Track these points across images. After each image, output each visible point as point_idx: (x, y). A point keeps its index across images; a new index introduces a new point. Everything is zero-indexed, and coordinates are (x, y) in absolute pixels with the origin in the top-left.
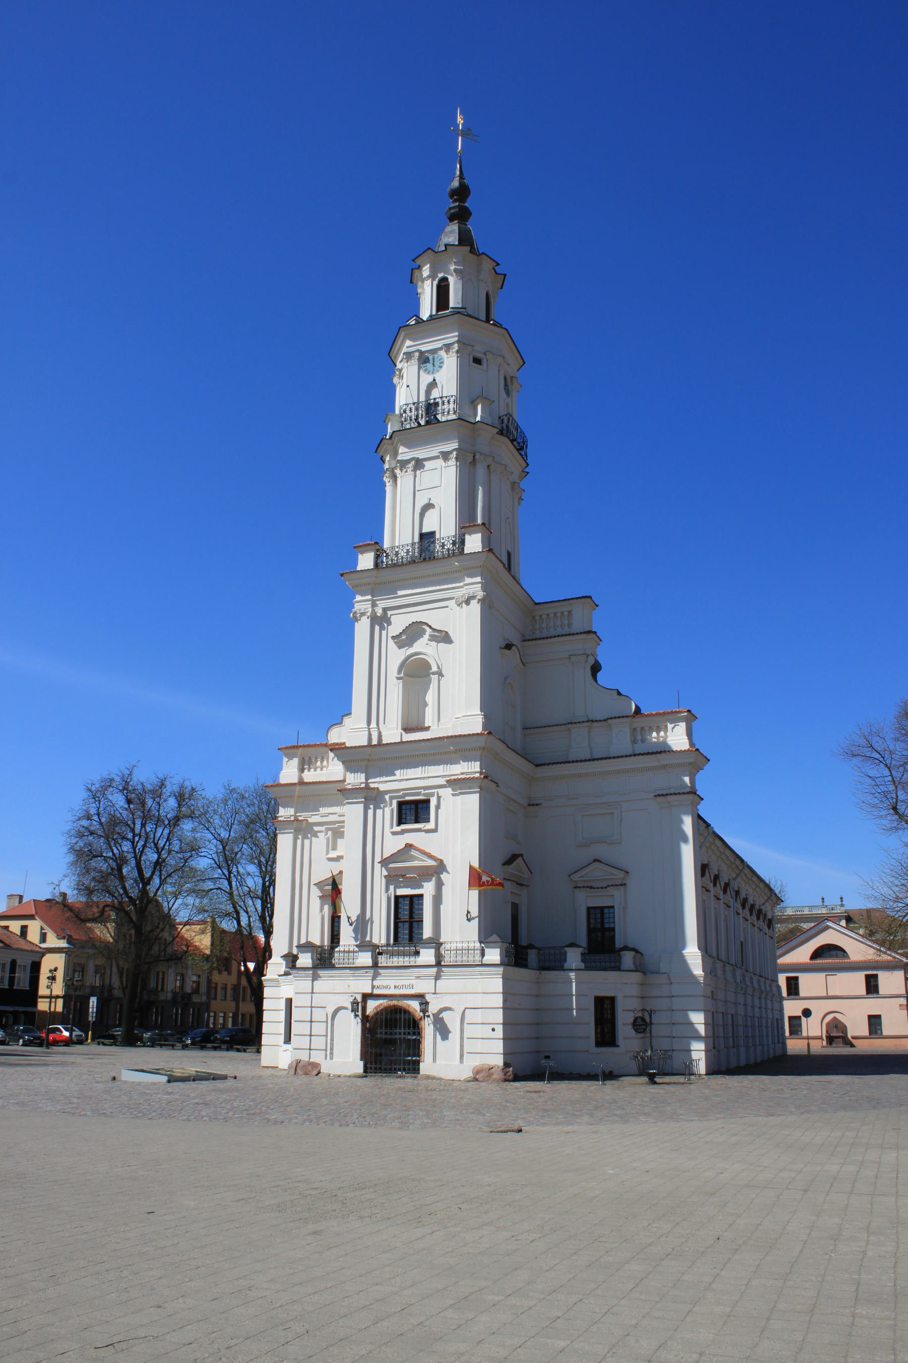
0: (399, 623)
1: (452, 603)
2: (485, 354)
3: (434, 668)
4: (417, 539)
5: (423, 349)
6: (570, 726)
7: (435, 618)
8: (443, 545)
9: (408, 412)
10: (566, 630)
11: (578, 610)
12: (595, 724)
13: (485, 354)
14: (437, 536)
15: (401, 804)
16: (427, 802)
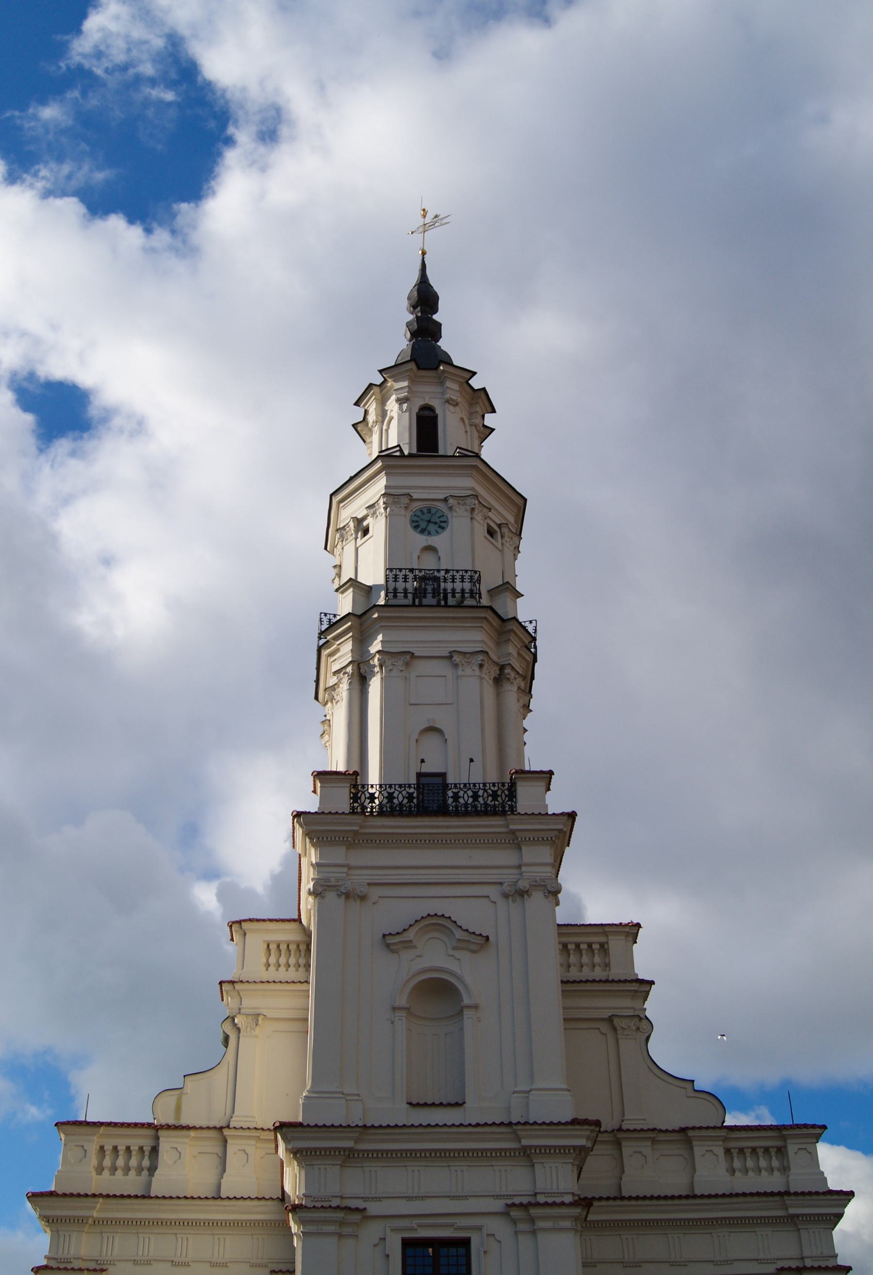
0: (396, 911)
1: (493, 892)
2: (499, 526)
3: (466, 1001)
4: (413, 780)
5: (415, 496)
6: (620, 1135)
7: (470, 913)
8: (456, 797)
9: (401, 580)
10: (599, 973)
11: (615, 944)
12: (662, 1137)
13: (499, 526)
14: (450, 780)
15: (408, 1244)
16: (465, 1243)
